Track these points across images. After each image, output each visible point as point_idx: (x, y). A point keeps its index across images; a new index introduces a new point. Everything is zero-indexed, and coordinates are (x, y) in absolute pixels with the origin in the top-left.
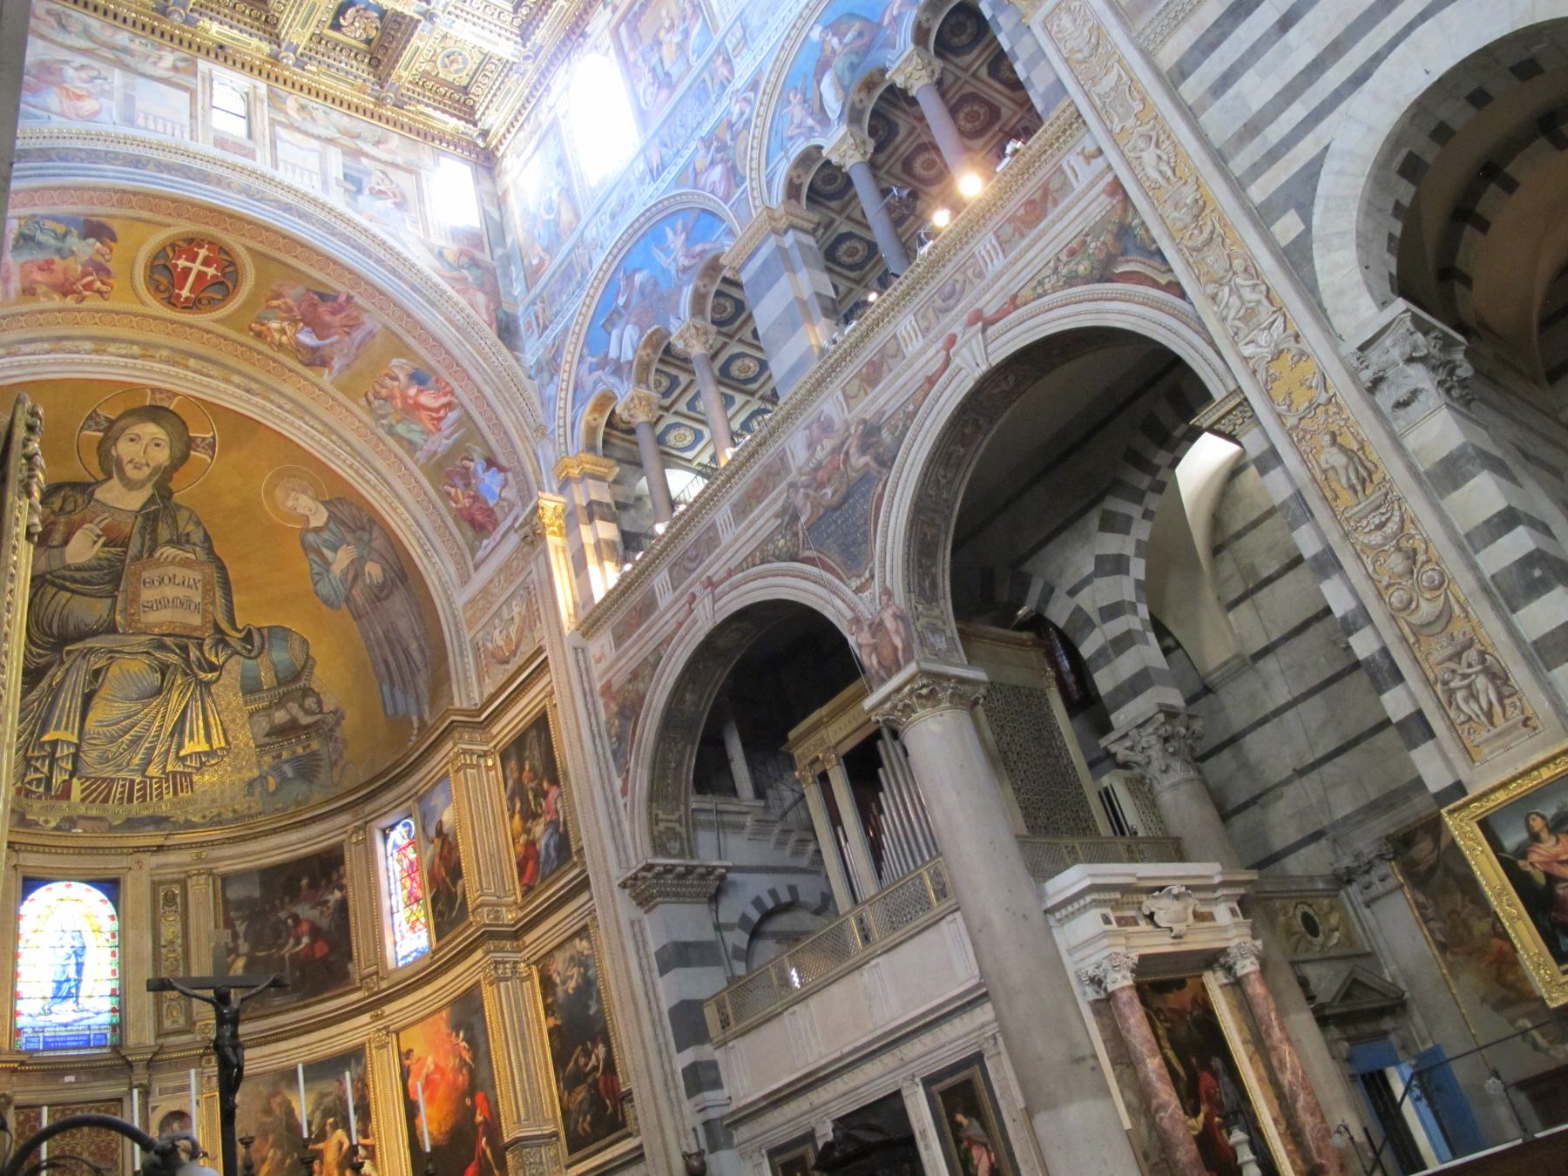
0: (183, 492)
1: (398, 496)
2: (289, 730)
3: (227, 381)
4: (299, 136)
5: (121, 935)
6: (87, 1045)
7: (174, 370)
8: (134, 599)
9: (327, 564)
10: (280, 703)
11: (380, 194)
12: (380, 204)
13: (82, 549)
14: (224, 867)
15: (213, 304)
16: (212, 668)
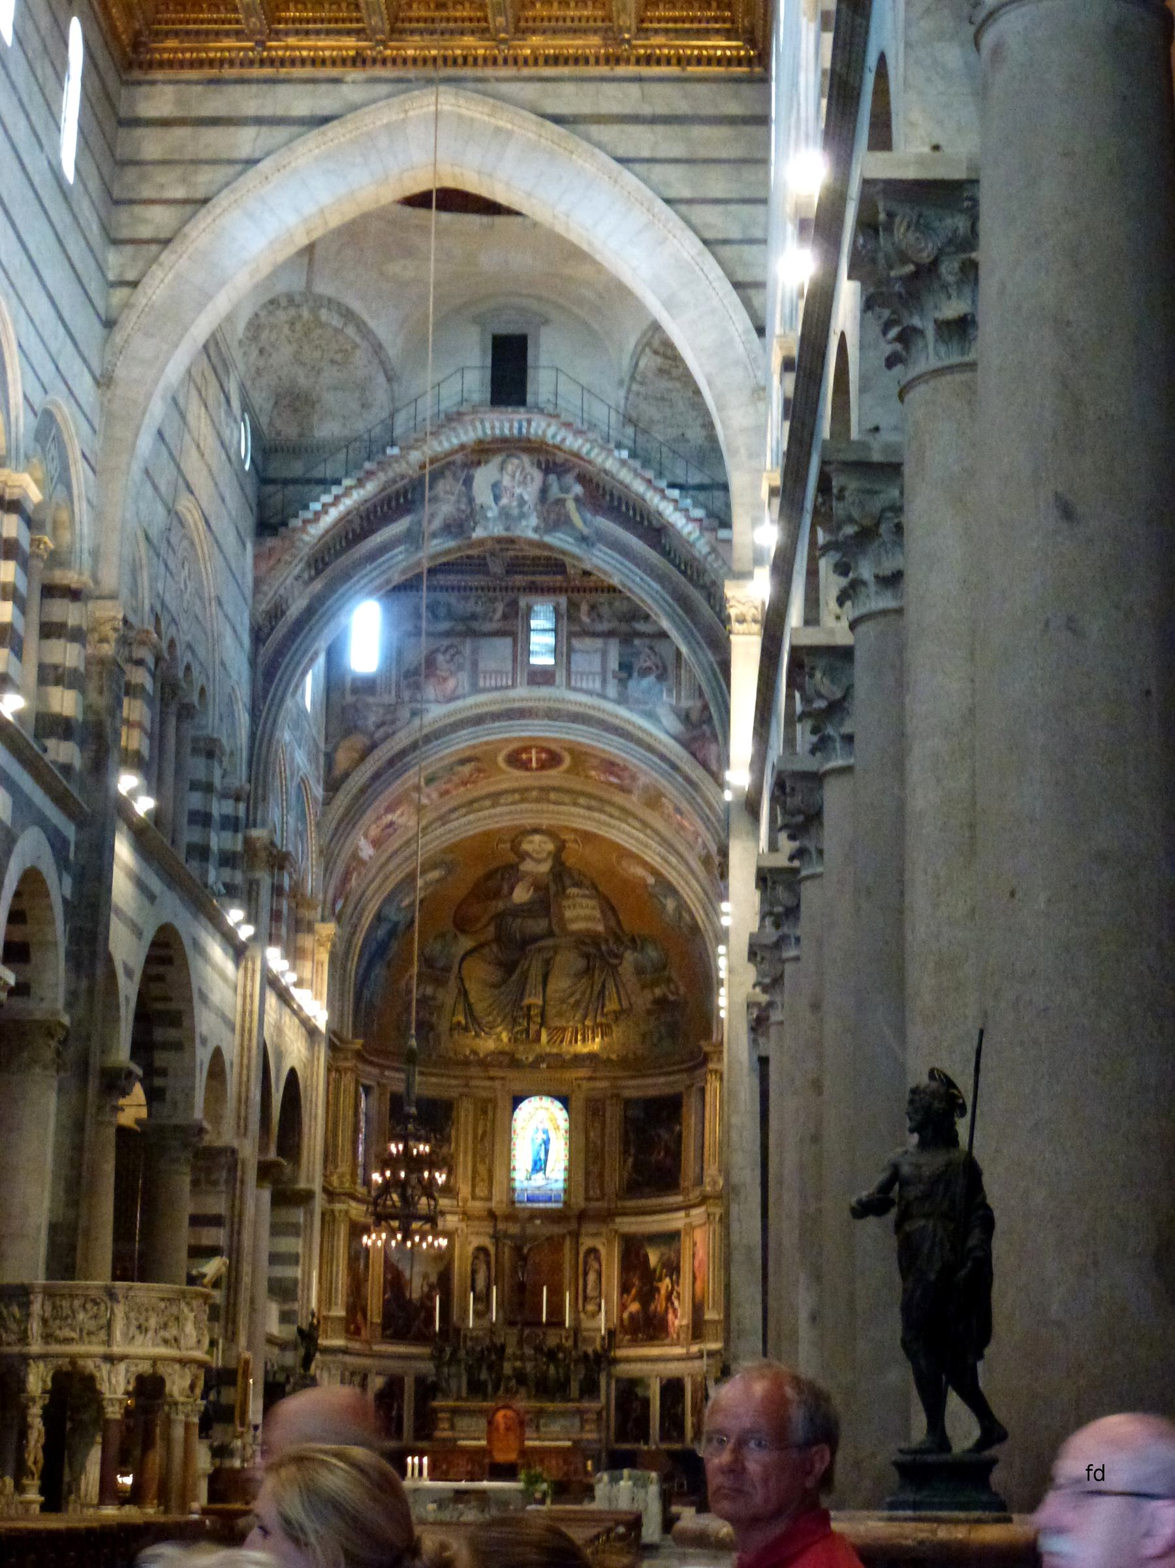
0: (570, 862)
1: (693, 872)
2: (661, 1003)
3: (575, 804)
4: (588, 642)
5: (571, 1131)
6: (549, 1200)
7: (539, 806)
8: (561, 918)
9: (664, 907)
10: (654, 984)
11: (645, 672)
12: (646, 682)
13: (521, 894)
14: (627, 1093)
15: (551, 766)
16: (616, 956)
